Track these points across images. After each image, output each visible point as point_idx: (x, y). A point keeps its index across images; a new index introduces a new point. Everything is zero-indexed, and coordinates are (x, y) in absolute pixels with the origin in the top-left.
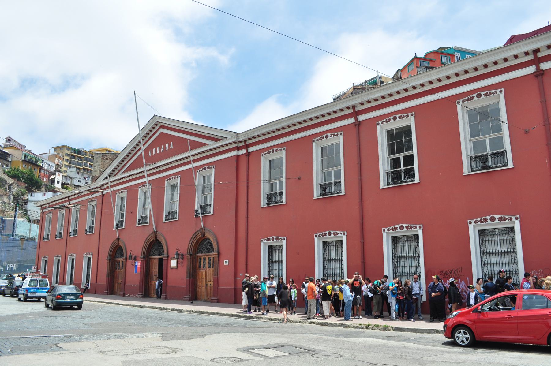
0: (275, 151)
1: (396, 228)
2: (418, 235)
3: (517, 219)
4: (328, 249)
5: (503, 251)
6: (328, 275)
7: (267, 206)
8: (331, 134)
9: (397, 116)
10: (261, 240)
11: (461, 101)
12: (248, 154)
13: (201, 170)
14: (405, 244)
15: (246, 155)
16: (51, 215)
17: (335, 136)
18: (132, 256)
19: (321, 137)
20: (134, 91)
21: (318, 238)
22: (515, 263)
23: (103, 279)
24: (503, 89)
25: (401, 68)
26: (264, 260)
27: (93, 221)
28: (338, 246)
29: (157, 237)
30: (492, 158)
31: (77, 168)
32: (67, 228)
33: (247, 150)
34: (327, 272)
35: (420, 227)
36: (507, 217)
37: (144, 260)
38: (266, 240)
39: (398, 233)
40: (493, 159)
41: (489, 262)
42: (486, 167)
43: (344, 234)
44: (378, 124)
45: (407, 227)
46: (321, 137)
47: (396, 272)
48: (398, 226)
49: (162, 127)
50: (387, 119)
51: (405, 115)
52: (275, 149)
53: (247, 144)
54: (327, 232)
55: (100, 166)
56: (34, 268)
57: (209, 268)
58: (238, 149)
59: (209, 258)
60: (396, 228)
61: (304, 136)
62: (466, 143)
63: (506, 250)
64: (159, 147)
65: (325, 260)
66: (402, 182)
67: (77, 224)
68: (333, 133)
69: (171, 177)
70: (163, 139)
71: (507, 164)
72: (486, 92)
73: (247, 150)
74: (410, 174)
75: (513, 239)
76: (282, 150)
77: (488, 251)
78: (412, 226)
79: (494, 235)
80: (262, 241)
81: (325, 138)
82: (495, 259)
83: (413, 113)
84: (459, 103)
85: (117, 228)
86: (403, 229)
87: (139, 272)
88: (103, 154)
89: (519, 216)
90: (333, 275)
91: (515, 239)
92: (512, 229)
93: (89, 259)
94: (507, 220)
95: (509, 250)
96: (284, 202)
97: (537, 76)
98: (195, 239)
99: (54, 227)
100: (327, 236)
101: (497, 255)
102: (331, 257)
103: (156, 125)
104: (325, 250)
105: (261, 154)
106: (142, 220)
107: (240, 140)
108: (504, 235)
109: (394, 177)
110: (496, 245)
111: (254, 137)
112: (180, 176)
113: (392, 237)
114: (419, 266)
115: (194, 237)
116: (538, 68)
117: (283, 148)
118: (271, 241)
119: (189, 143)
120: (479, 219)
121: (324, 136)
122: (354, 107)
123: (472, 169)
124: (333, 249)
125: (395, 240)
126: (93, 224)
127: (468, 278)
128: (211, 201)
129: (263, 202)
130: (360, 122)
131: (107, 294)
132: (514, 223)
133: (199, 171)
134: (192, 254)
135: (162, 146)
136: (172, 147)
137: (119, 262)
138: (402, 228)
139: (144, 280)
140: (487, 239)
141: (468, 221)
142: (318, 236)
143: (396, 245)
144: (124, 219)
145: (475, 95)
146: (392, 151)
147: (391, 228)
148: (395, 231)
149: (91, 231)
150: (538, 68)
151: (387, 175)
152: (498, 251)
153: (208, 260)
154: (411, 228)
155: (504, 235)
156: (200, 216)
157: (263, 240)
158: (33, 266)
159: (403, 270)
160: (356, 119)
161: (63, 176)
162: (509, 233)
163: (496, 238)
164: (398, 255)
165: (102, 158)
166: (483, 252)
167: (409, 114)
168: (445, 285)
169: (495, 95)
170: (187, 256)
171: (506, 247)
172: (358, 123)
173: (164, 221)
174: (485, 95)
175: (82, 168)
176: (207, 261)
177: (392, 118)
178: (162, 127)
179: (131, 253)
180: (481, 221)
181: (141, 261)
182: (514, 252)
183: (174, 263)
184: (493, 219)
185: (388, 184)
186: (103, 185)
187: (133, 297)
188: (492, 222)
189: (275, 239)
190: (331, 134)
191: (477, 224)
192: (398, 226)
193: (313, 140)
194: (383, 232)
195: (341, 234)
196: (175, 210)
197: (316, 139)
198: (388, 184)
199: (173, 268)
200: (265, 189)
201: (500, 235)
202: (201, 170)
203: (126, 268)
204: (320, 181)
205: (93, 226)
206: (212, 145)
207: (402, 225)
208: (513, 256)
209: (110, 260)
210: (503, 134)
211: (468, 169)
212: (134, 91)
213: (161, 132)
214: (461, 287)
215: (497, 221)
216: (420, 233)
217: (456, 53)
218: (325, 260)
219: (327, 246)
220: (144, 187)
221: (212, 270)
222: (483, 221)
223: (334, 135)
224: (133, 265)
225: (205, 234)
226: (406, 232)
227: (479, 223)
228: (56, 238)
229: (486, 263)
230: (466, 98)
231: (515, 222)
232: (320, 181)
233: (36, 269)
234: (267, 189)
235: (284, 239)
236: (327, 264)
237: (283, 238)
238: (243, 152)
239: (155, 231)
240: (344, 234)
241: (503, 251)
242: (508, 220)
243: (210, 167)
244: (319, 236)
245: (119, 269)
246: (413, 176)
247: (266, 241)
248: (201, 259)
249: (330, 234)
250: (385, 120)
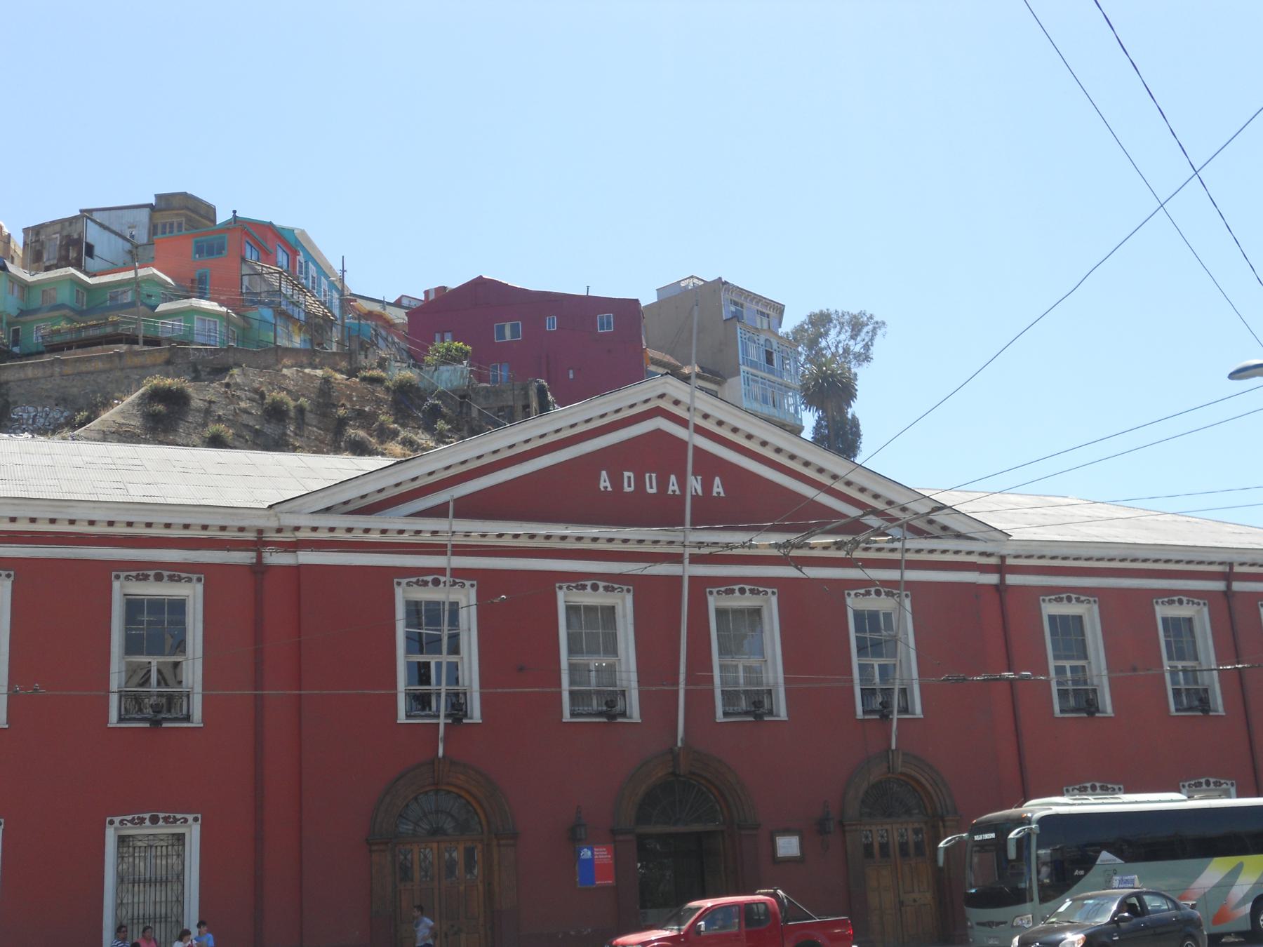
12: (1000, 588)
13: (863, 595)
38: (1078, 789)
64: (654, 475)
68: (1191, 599)
112: (775, 590)
122: (1231, 565)
160: (1229, 586)
189: (1098, 789)
190: (1188, 598)
195: (1227, 784)
202: (863, 595)
223: (1193, 603)
238: (992, 579)
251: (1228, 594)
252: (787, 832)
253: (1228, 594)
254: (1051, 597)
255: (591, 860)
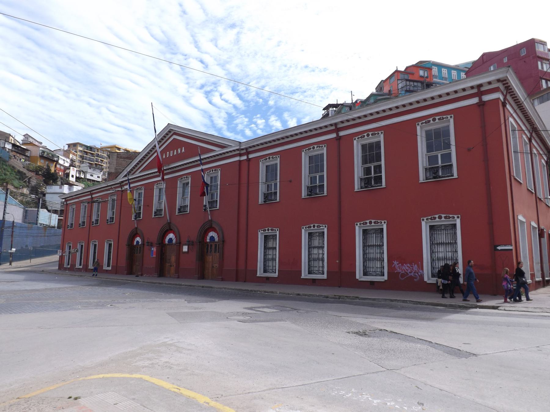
0: (271, 158)
1: (366, 223)
2: (383, 229)
3: (458, 217)
4: (312, 239)
5: (447, 242)
6: (312, 259)
7: (263, 203)
8: (317, 146)
9: (370, 133)
10: (259, 230)
11: (420, 123)
13: (209, 172)
14: (372, 236)
15: (247, 161)
16: (74, 207)
17: (320, 148)
18: (149, 242)
19: (309, 148)
20: (152, 103)
21: (305, 230)
22: (456, 251)
23: (123, 262)
24: (453, 116)
25: (384, 79)
26: (261, 246)
27: (113, 212)
28: (321, 236)
29: (171, 227)
30: (442, 169)
31: (89, 163)
32: (89, 218)
33: (248, 157)
34: (311, 257)
35: (385, 223)
36: (451, 216)
37: (159, 246)
39: (368, 227)
40: (443, 170)
41: (436, 251)
42: (436, 176)
43: (325, 227)
44: (355, 139)
45: (375, 223)
46: (309, 148)
47: (366, 257)
48: (368, 221)
49: (175, 134)
50: (362, 135)
51: (376, 132)
52: (271, 157)
53: (248, 151)
54: (312, 225)
55: (115, 164)
56: (59, 252)
57: (215, 252)
58: (240, 155)
59: (215, 245)
60: (366, 223)
61: (295, 146)
62: (422, 157)
63: (449, 242)
65: (310, 247)
66: (372, 187)
67: (98, 215)
68: (318, 145)
69: (183, 177)
70: (176, 144)
71: (453, 175)
72: (439, 117)
73: (248, 157)
74: (378, 179)
75: (455, 233)
76: (276, 157)
77: (436, 242)
78: (379, 221)
79: (441, 230)
80: (259, 231)
81: (312, 149)
82: (441, 249)
83: (383, 131)
84: (418, 124)
85: (135, 219)
86: (372, 223)
87: (154, 256)
88: (118, 153)
89: (460, 216)
90: (316, 259)
91: (456, 233)
92: (455, 225)
93: (110, 245)
94: (451, 219)
95: (452, 242)
96: (278, 200)
97: (479, 106)
98: (203, 229)
99: (77, 217)
100: (312, 228)
101: (443, 245)
102: (315, 245)
103: (170, 132)
104: (310, 239)
105: (260, 160)
106: (158, 212)
107: (242, 148)
108: (449, 230)
109: (366, 182)
110: (442, 237)
111: (254, 146)
113: (363, 230)
114: (383, 253)
115: (203, 227)
116: (480, 99)
117: (277, 156)
118: (267, 231)
119: (199, 149)
120: (430, 217)
121: (312, 147)
122: (336, 124)
123: (426, 178)
124: (316, 238)
125: (365, 232)
126: (113, 215)
127: (420, 263)
128: (217, 198)
129: (261, 200)
130: (340, 137)
131: (127, 274)
132: (456, 220)
133: (207, 173)
134: (201, 241)
135: (175, 150)
136: (184, 151)
137: (137, 248)
138: (370, 223)
139: (159, 262)
140: (435, 233)
141: (422, 219)
142: (304, 228)
143: (366, 236)
144: (142, 211)
145: (431, 119)
146: (365, 161)
147: (362, 222)
148: (365, 225)
149: (111, 220)
150: (480, 99)
151: (361, 180)
152: (444, 242)
153: (214, 246)
154: (378, 223)
155: (449, 230)
156: (208, 210)
157: (260, 230)
158: (58, 251)
159: (372, 256)
160: (338, 135)
161: (77, 170)
162: (452, 229)
163: (442, 232)
164: (367, 244)
165: (117, 157)
166: (433, 242)
167: (379, 132)
168: (402, 267)
169: (446, 119)
170: (197, 243)
171: (449, 240)
172: (339, 138)
173: (177, 214)
174: (439, 119)
175: (94, 163)
176: (213, 247)
177: (365, 134)
178: (175, 134)
179: (148, 240)
180: (431, 219)
181: (157, 246)
182: (456, 243)
183: (185, 249)
184: (440, 217)
185: (361, 188)
186: (122, 182)
187: (149, 276)
188: (439, 220)
189: (270, 230)
190: (317, 146)
191: (428, 221)
192: (368, 221)
193: (302, 150)
194: (356, 225)
195: (323, 227)
196: (186, 204)
197: (305, 149)
198: (361, 188)
199: (185, 253)
200: (262, 189)
201: (445, 230)
202: (209, 172)
203: (143, 253)
204: (307, 184)
205: (114, 217)
206: (219, 151)
207: (370, 220)
208: (454, 246)
209: (129, 245)
210: (451, 150)
211: (423, 178)
212: (152, 103)
213: (174, 138)
214: (414, 269)
215: (443, 219)
216: (385, 227)
217: (433, 67)
218: (310, 247)
219: (312, 236)
220: (159, 184)
221: (218, 254)
222: (433, 219)
223: (319, 147)
224: (150, 250)
225: (212, 225)
226: (374, 226)
227: (430, 220)
228: (80, 226)
229: (434, 251)
230: (424, 121)
231: (457, 220)
232: (307, 184)
233: (61, 253)
234: (264, 189)
235: (278, 230)
236: (311, 250)
237: (276, 229)
238: (244, 158)
239: (169, 221)
240: (325, 227)
241: (447, 242)
242: (452, 218)
243: (217, 169)
244: (306, 228)
245: (137, 253)
246: (381, 182)
247: (262, 232)
248: (208, 245)
249: (314, 226)
250: (360, 136)
251: (339, 138)
252: (185, 245)
253: (339, 138)
254: (263, 159)
255: (153, 250)
